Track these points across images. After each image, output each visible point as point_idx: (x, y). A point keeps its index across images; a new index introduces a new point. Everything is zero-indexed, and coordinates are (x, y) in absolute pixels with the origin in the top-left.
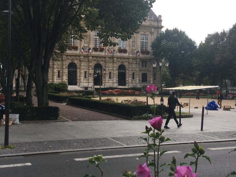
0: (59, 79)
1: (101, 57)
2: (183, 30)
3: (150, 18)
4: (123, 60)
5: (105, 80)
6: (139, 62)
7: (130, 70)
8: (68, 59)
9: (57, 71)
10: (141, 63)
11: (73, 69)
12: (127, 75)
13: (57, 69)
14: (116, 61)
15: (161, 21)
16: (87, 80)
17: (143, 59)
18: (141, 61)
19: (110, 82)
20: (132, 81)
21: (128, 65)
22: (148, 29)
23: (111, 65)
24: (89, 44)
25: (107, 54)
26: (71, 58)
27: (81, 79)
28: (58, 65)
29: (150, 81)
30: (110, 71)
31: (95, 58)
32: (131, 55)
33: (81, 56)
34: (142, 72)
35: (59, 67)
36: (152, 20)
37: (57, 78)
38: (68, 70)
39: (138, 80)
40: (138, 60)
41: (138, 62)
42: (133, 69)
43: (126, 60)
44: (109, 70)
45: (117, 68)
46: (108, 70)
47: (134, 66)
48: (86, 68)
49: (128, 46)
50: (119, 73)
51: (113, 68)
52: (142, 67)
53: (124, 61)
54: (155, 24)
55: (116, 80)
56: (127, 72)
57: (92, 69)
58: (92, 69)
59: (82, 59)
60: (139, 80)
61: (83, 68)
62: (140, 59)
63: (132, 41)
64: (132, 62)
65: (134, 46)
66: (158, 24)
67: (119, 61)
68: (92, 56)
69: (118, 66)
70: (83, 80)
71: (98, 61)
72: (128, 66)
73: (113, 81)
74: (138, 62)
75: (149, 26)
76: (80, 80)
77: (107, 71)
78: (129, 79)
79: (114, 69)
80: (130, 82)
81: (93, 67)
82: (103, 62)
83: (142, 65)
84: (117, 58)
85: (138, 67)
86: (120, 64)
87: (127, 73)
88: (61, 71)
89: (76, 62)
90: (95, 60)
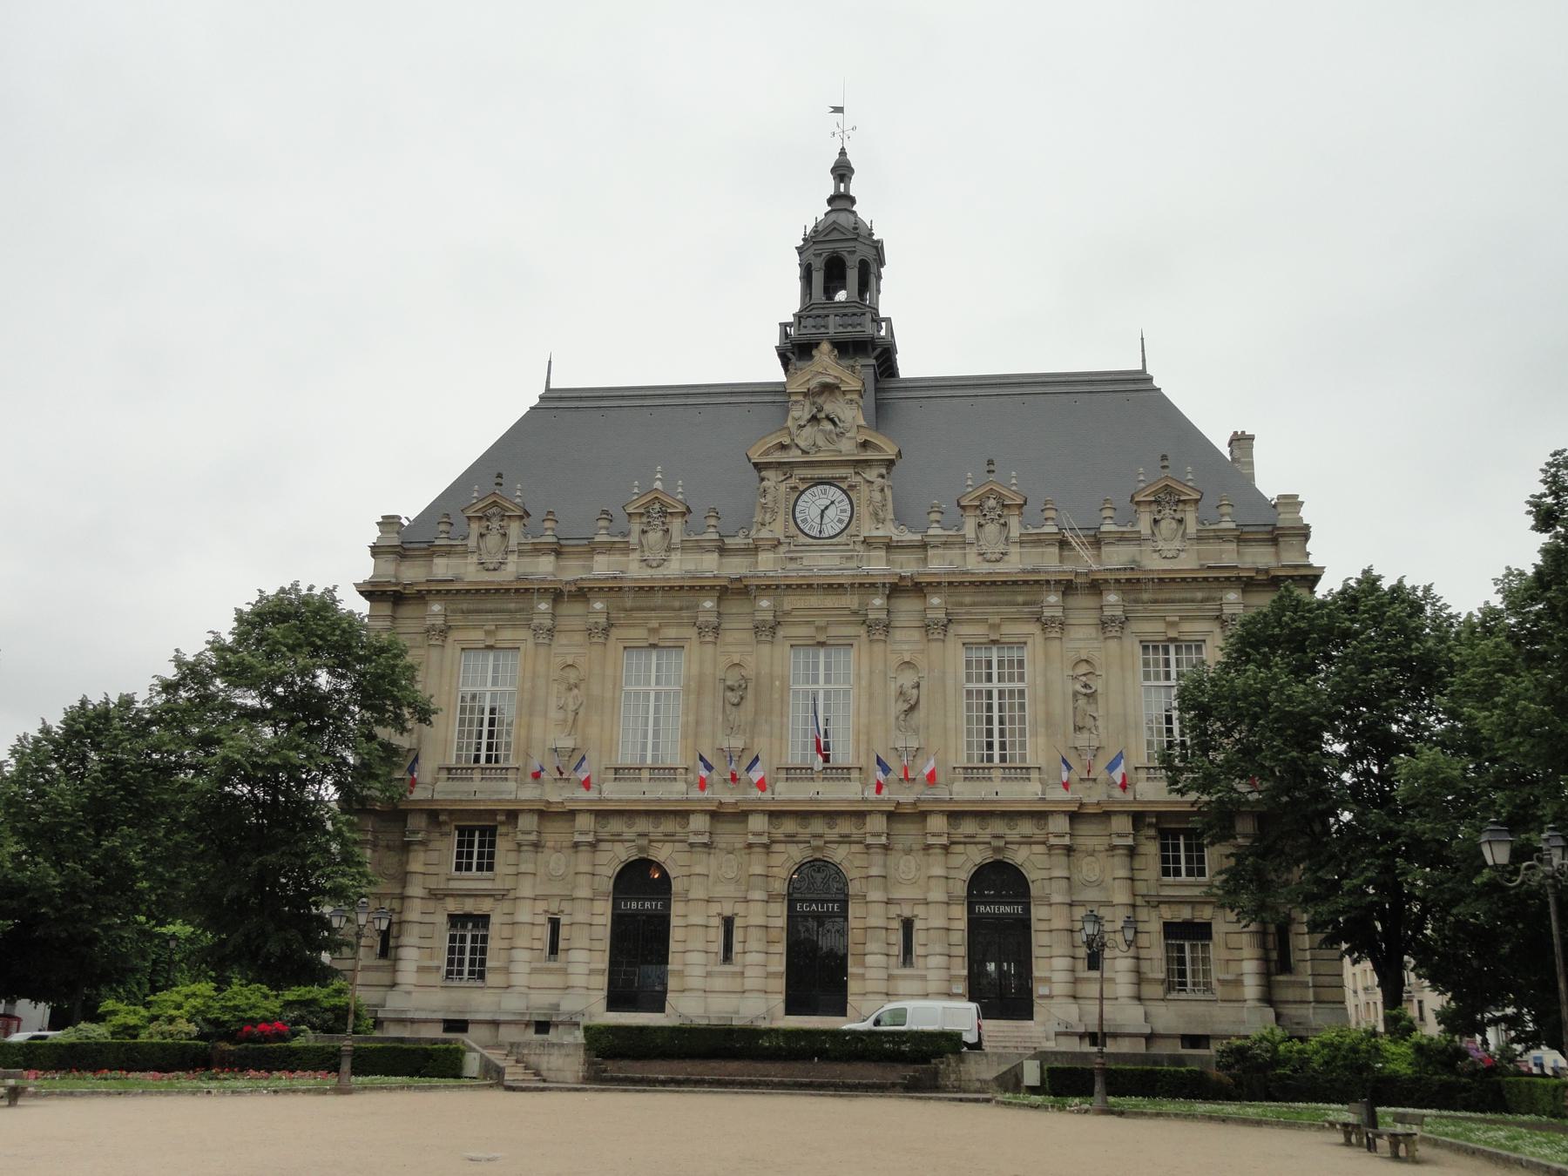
0: (549, 971)
1: (831, 816)
2: (1415, 580)
3: (1200, 521)
4: (998, 827)
5: (862, 977)
6: (1130, 841)
7: (1056, 898)
8: (617, 838)
9: (543, 919)
10: (1151, 849)
11: (647, 905)
12: (1039, 939)
13: (541, 906)
14: (944, 840)
15: (1304, 533)
16: (734, 974)
17: (1159, 814)
18: (1152, 832)
19: (903, 986)
20: (1076, 981)
21: (1042, 861)
22: (1193, 601)
23: (913, 864)
24: (752, 738)
25: (871, 794)
26: (629, 833)
27: (688, 970)
28: (551, 878)
29: (1238, 982)
30: (907, 912)
31: (789, 826)
32: (1060, 794)
33: (693, 812)
34: (1168, 914)
35: (555, 891)
36: (1220, 537)
37: (539, 965)
38: (615, 906)
39: (1131, 977)
40: (1123, 824)
41: (1119, 835)
42: (1091, 895)
43: (1026, 827)
44: (898, 902)
45: (961, 890)
46: (888, 902)
47: (1089, 869)
48: (730, 890)
49: (1041, 730)
50: (975, 923)
51: (928, 890)
52: (1166, 872)
53: (1013, 834)
54: (1259, 558)
55: (943, 974)
56: (1037, 912)
57: (771, 898)
58: (771, 898)
59: (696, 833)
60: (1140, 978)
61: (702, 895)
62: (1138, 818)
63: (1076, 694)
64: (1066, 841)
65: (1089, 722)
66: (1277, 554)
67: (970, 840)
68: (763, 812)
69: (965, 875)
70: (709, 975)
71: (814, 843)
72: (1044, 874)
73: (924, 978)
74: (1118, 841)
75: (1195, 579)
76: (681, 974)
77: (878, 909)
78: (1052, 966)
79: (932, 896)
80: (1060, 988)
81: (780, 887)
82: (856, 848)
83: (1165, 860)
84: (954, 816)
85: (1122, 873)
86: (978, 860)
87: (1043, 926)
88: (564, 920)
89: (661, 853)
90: (791, 839)
